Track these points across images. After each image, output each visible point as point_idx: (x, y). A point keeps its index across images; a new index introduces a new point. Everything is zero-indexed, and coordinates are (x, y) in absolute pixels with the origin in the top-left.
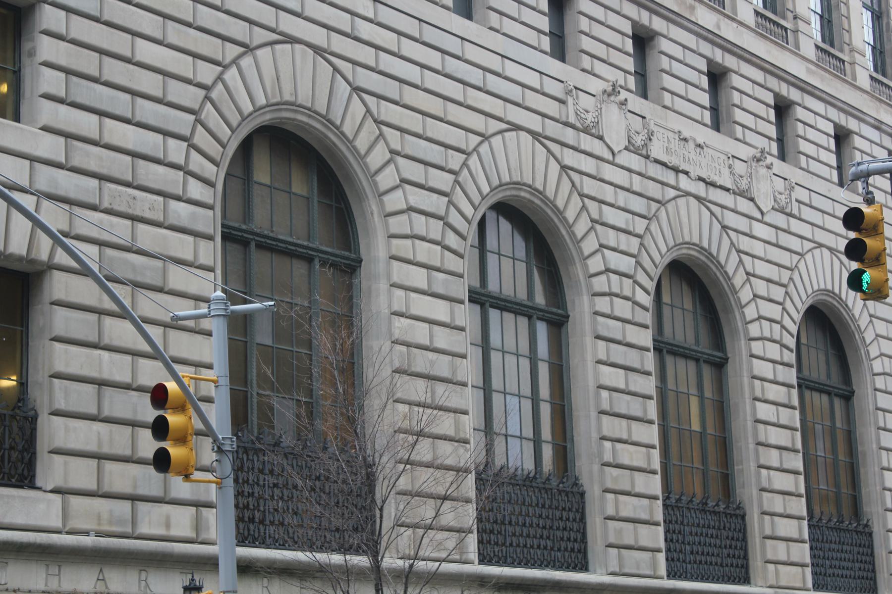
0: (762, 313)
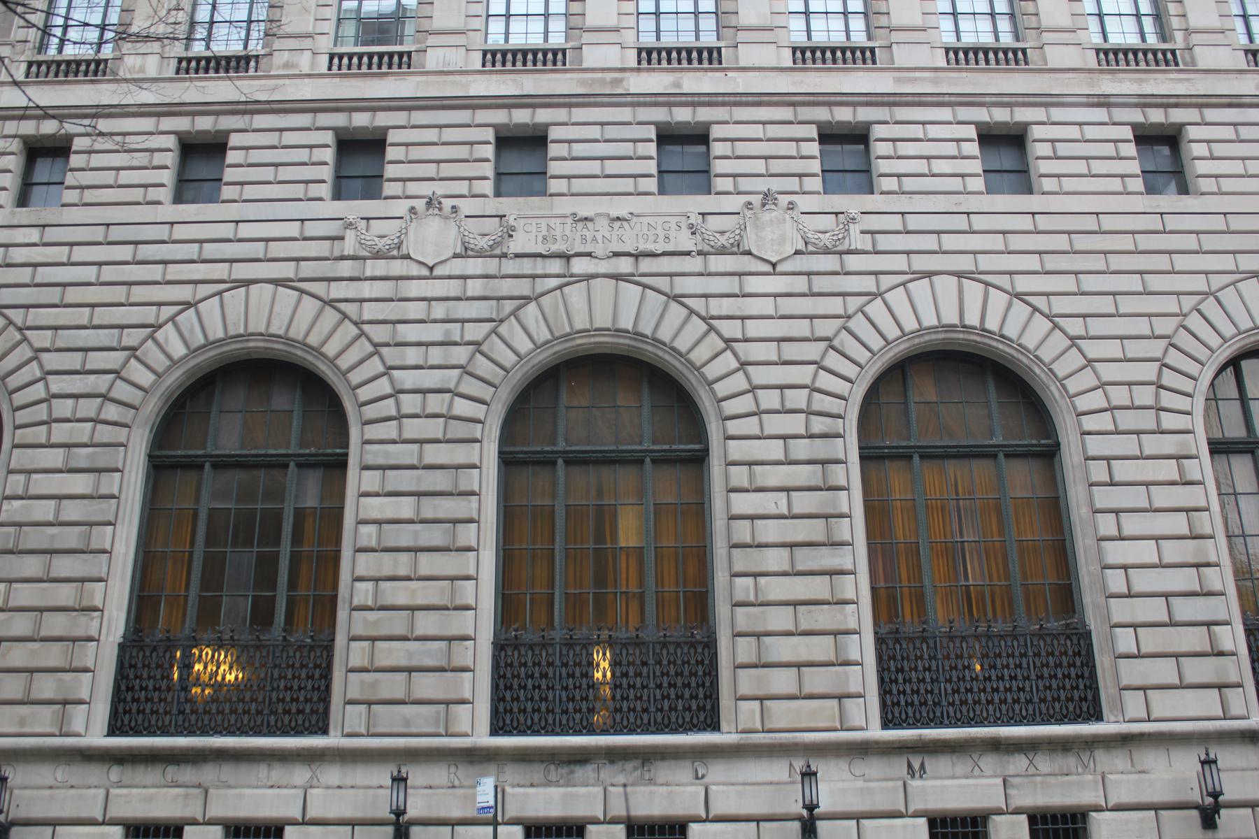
0: (757, 381)
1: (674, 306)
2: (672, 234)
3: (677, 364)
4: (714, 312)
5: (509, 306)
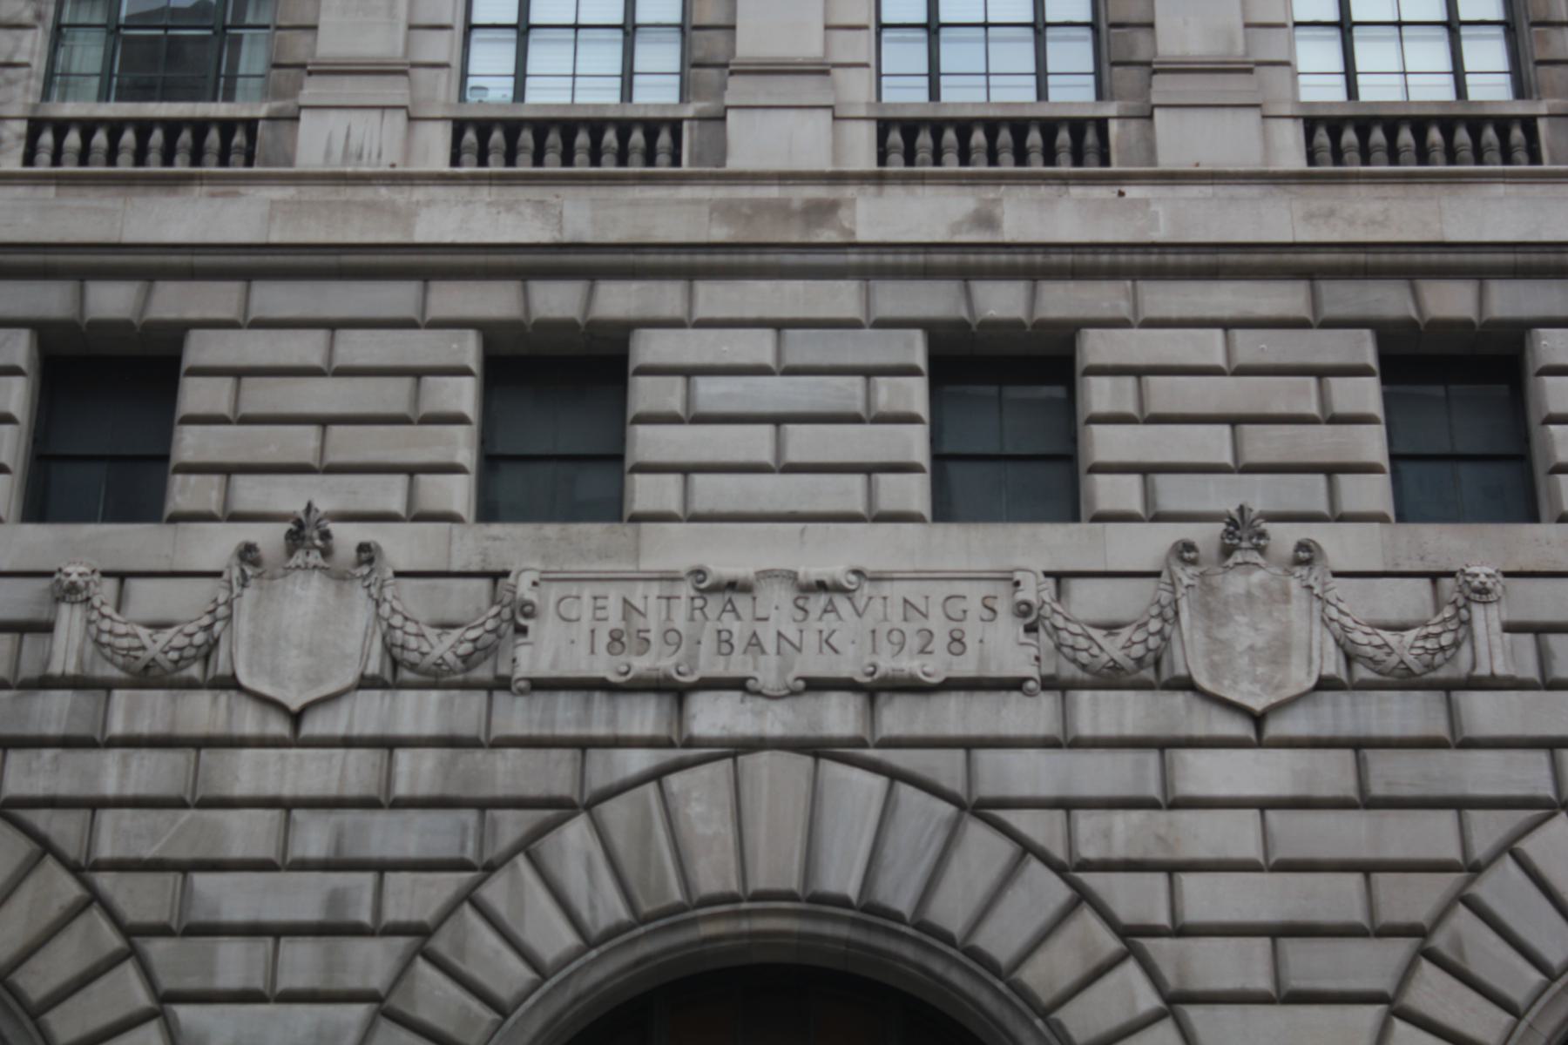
1: (977, 833)
2: (972, 631)
3: (986, 998)
4: (1089, 852)
5: (512, 825)
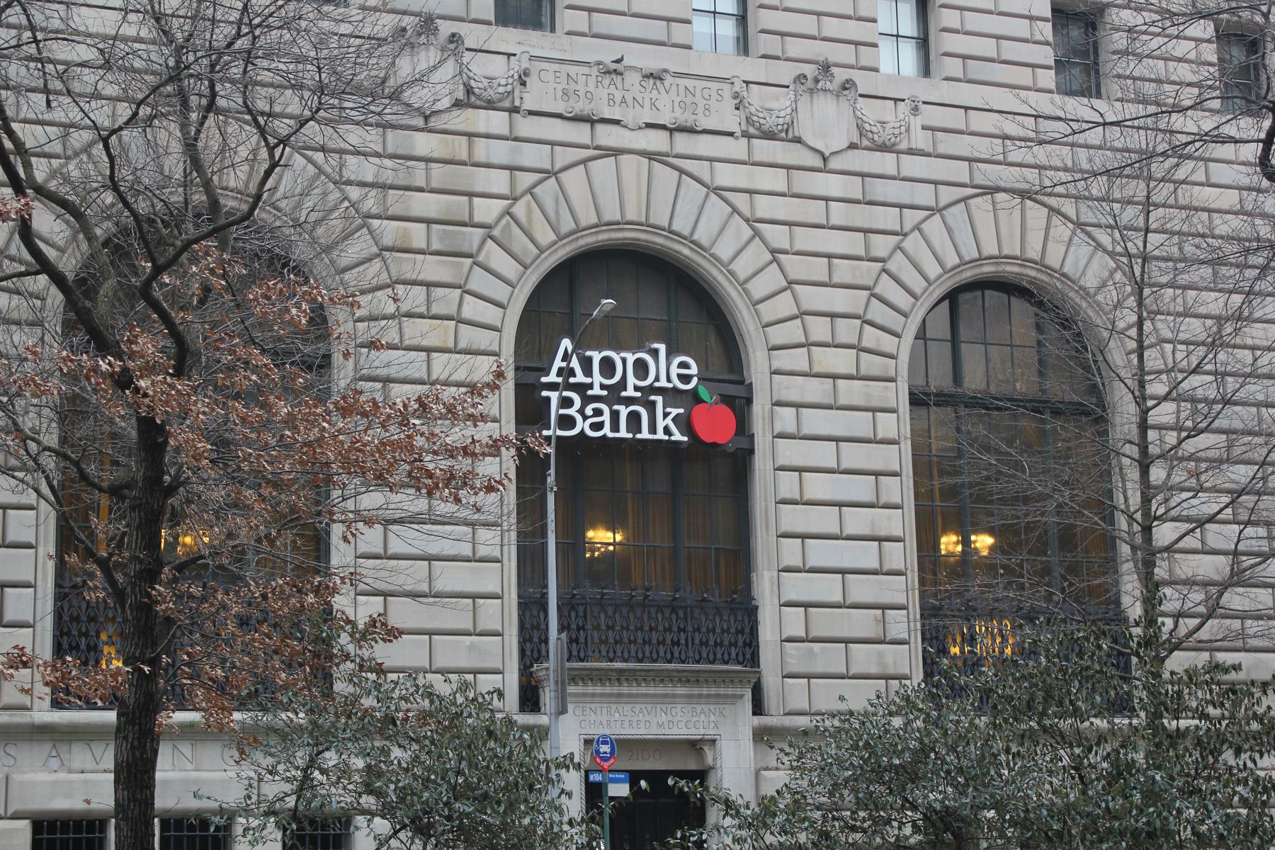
0: (806, 306)
4: (760, 214)
5: (527, 179)
